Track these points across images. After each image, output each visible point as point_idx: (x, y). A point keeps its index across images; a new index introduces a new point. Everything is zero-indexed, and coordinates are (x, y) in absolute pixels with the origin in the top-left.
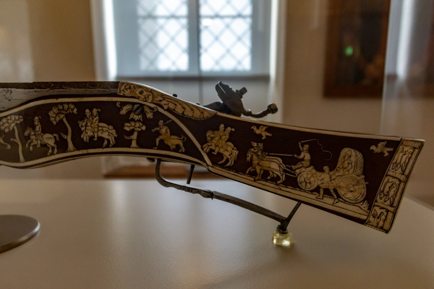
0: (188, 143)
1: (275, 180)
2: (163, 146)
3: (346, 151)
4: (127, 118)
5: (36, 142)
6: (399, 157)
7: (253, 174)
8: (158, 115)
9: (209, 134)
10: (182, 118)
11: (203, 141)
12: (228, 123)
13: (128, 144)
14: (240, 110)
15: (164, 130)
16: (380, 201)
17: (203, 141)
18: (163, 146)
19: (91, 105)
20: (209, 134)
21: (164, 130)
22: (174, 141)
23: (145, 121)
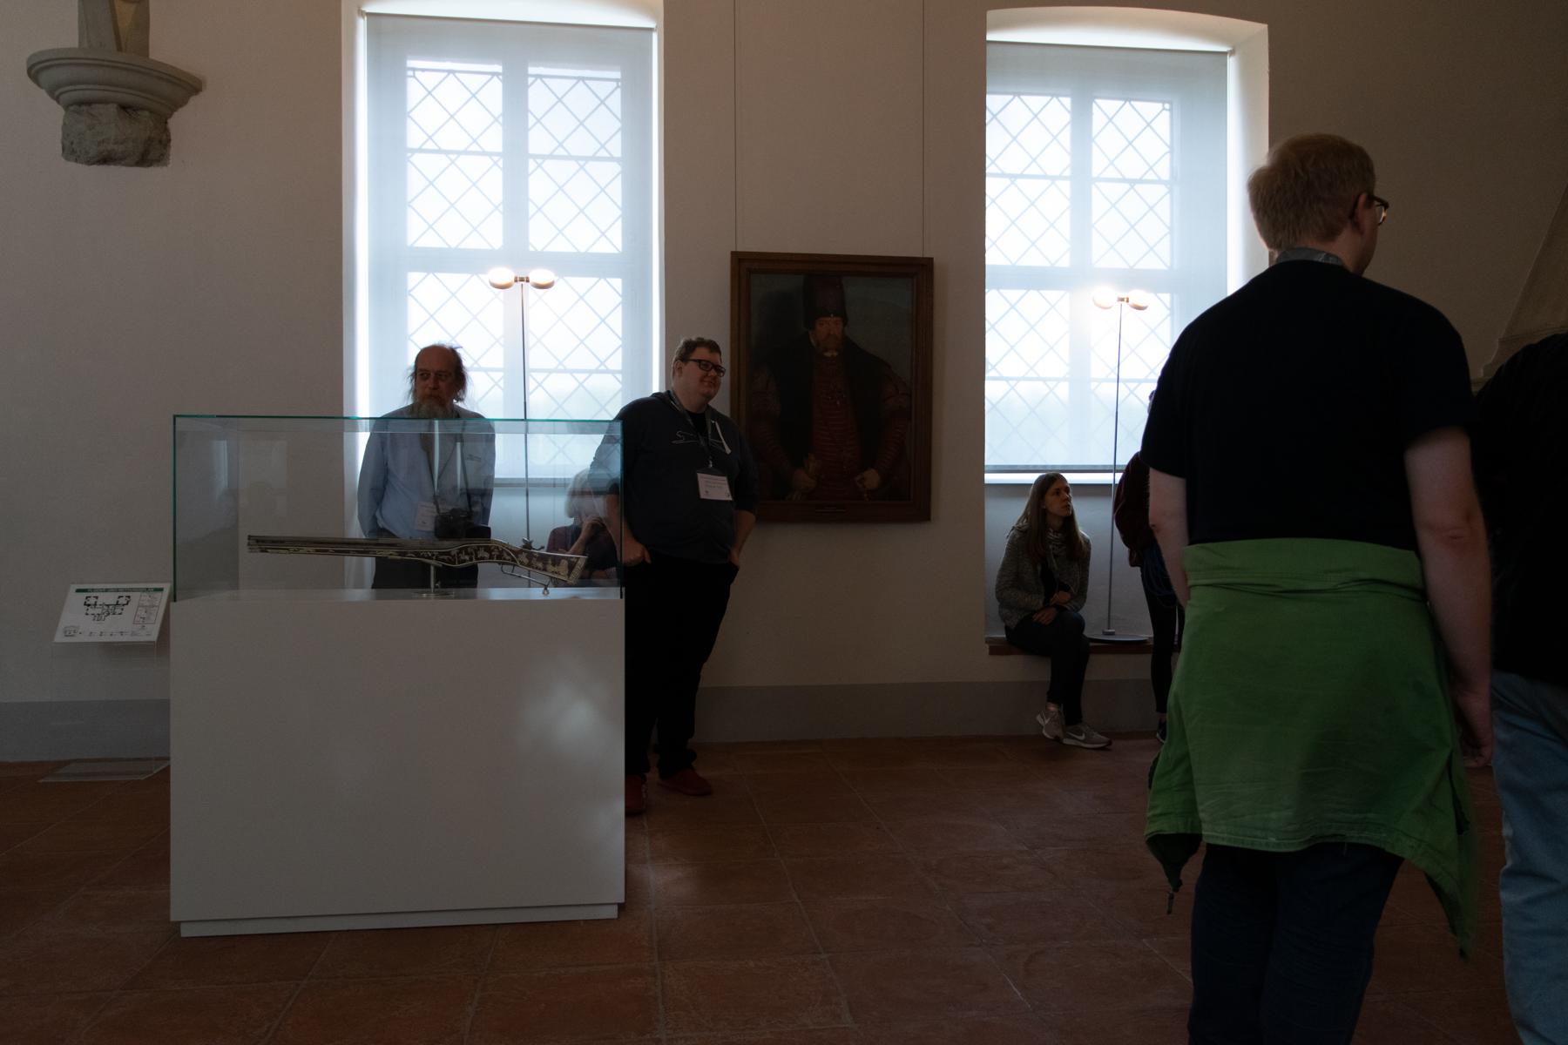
0: (512, 558)
1: (540, 569)
2: (505, 559)
3: (563, 561)
4: (493, 551)
5: (462, 558)
6: (579, 562)
7: (533, 567)
8: (503, 550)
9: (519, 555)
10: (513, 551)
11: (517, 557)
12: (525, 552)
13: (493, 559)
14: (531, 548)
15: (505, 555)
16: (572, 575)
17: (517, 557)
18: (505, 559)
19: (481, 546)
20: (519, 555)
21: (505, 555)
22: (508, 558)
23: (499, 551)
